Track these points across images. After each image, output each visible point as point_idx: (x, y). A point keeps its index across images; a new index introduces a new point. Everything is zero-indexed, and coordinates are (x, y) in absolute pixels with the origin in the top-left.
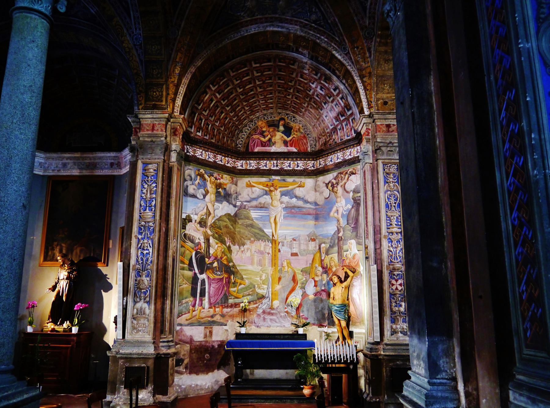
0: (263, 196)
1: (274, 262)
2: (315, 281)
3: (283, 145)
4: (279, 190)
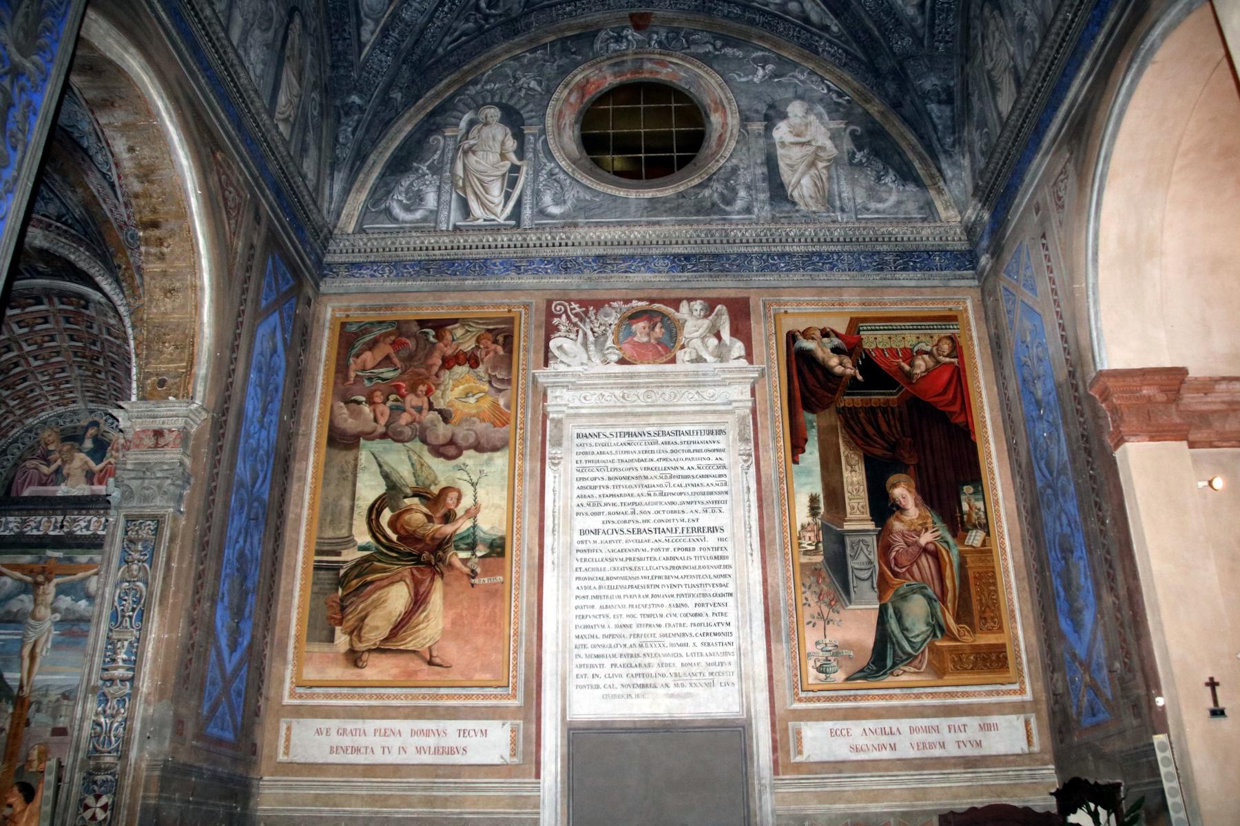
0: (18, 594)
3: (84, 479)
4: (56, 581)
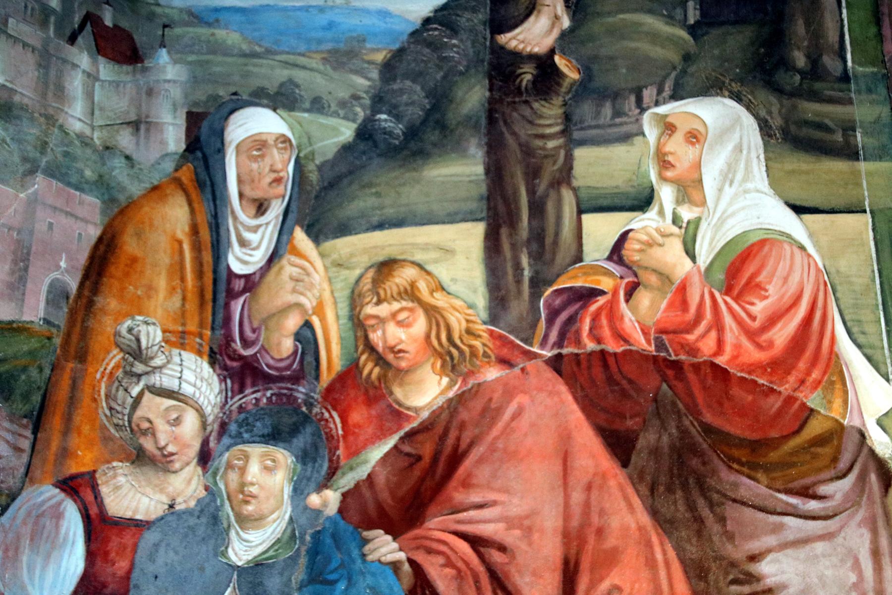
2: (100, 528)
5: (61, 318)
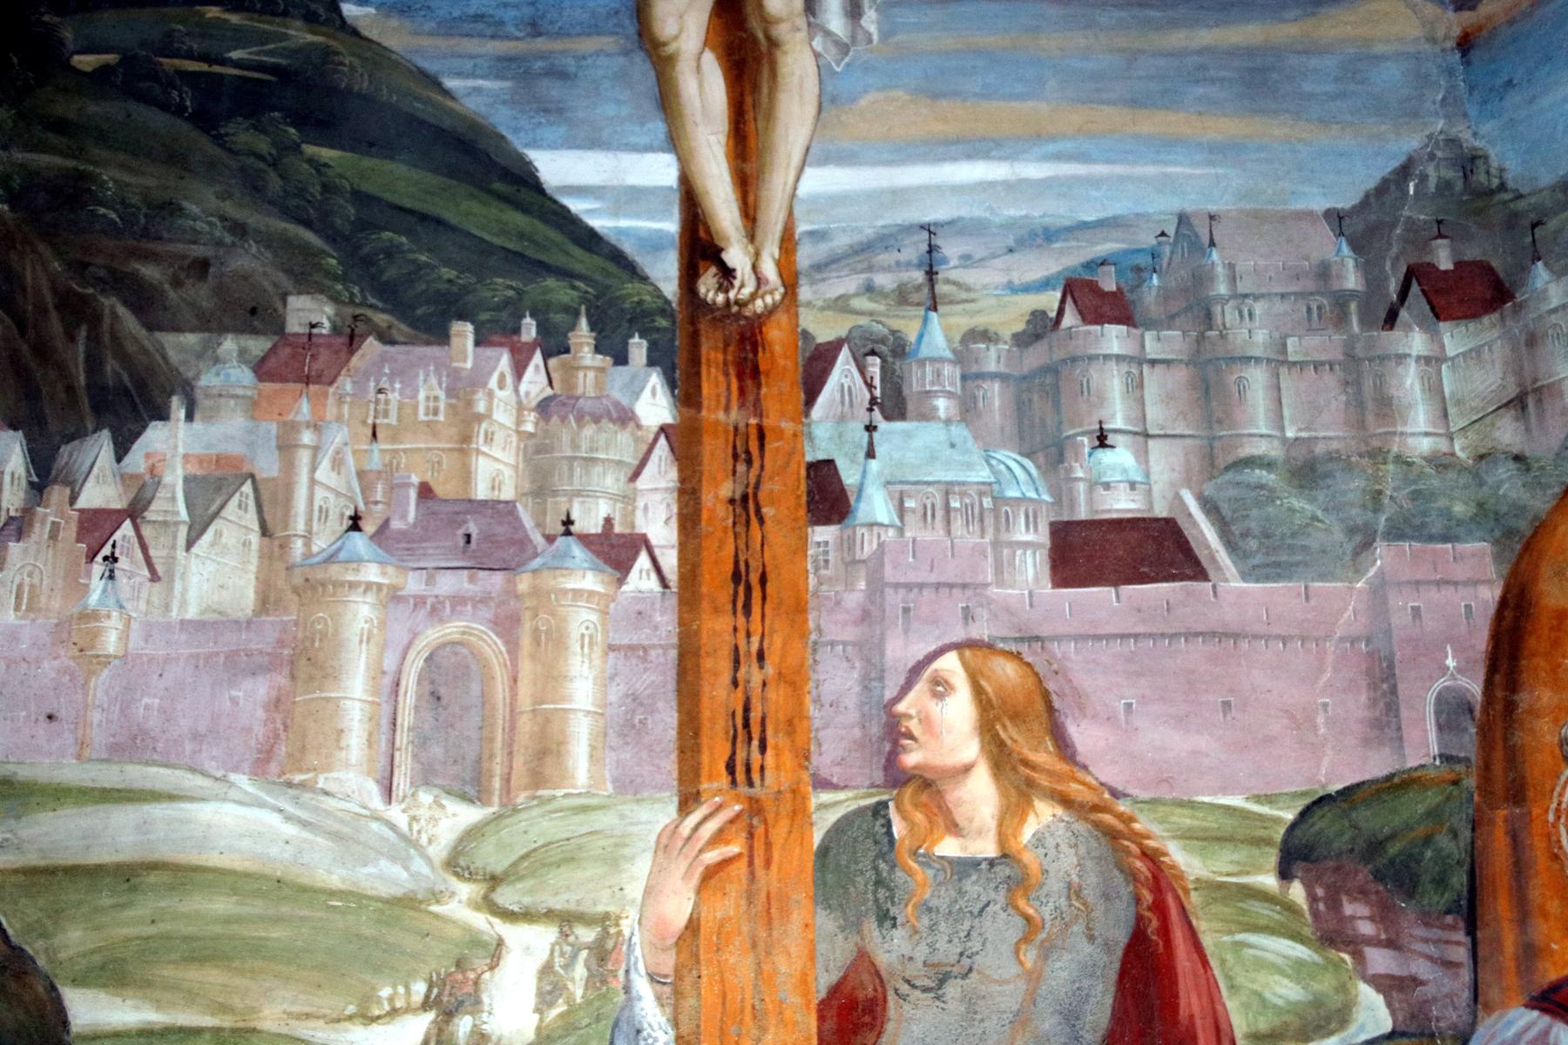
1: (718, 695)
5: (1468, 744)
